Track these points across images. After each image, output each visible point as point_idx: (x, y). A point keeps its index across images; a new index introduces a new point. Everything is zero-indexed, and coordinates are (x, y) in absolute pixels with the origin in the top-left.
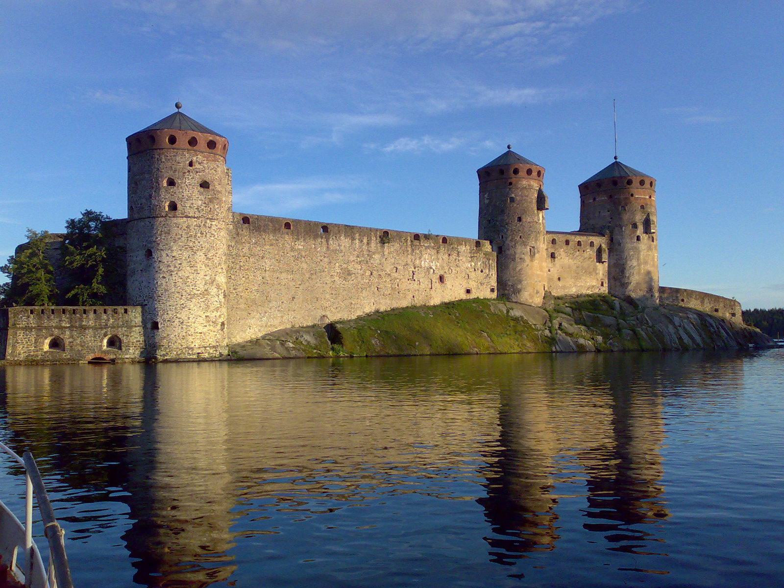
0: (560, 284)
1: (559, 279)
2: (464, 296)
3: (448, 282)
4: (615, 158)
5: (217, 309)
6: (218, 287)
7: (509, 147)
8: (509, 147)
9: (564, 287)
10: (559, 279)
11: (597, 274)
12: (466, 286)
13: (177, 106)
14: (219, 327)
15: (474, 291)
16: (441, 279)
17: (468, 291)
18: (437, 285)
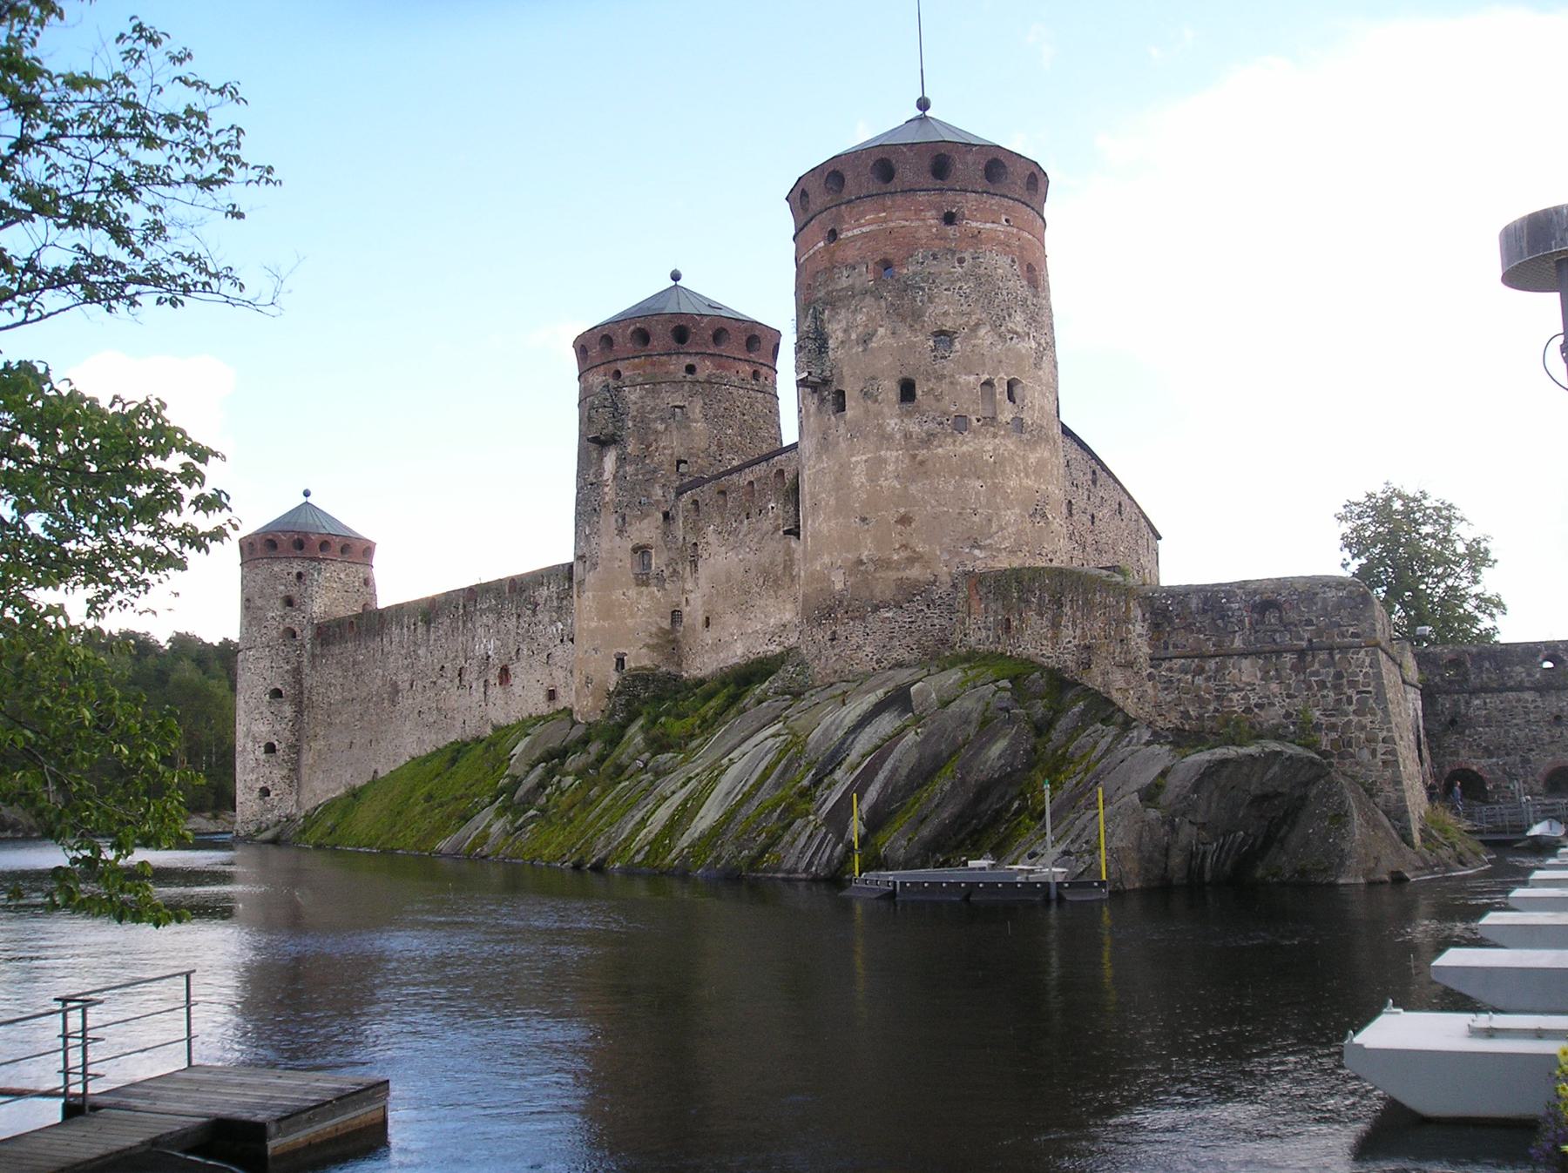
0: (708, 637)
1: (707, 623)
2: (544, 708)
3: (516, 682)
4: (923, 104)
5: (252, 771)
6: (254, 739)
7: (676, 276)
8: (676, 276)
9: (718, 645)
10: (707, 623)
11: (792, 579)
12: (547, 682)
13: (307, 494)
14: (256, 794)
15: (561, 692)
16: (504, 675)
17: (552, 695)
18: (496, 691)
